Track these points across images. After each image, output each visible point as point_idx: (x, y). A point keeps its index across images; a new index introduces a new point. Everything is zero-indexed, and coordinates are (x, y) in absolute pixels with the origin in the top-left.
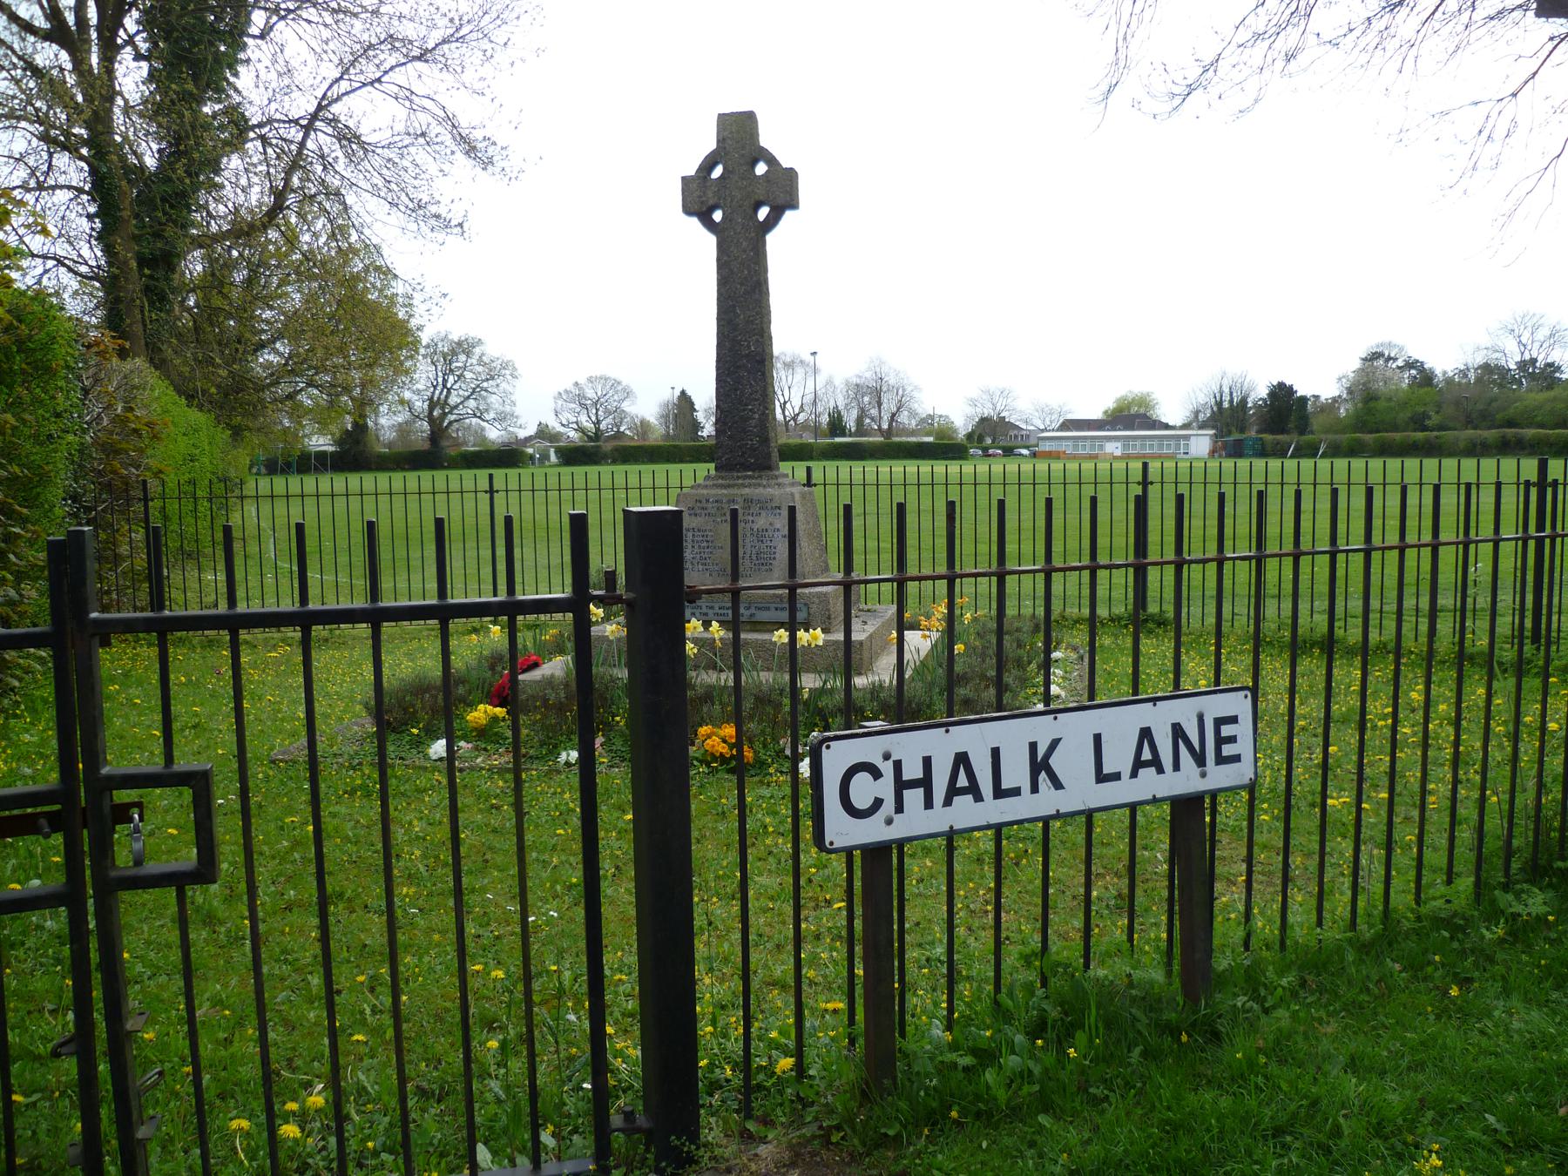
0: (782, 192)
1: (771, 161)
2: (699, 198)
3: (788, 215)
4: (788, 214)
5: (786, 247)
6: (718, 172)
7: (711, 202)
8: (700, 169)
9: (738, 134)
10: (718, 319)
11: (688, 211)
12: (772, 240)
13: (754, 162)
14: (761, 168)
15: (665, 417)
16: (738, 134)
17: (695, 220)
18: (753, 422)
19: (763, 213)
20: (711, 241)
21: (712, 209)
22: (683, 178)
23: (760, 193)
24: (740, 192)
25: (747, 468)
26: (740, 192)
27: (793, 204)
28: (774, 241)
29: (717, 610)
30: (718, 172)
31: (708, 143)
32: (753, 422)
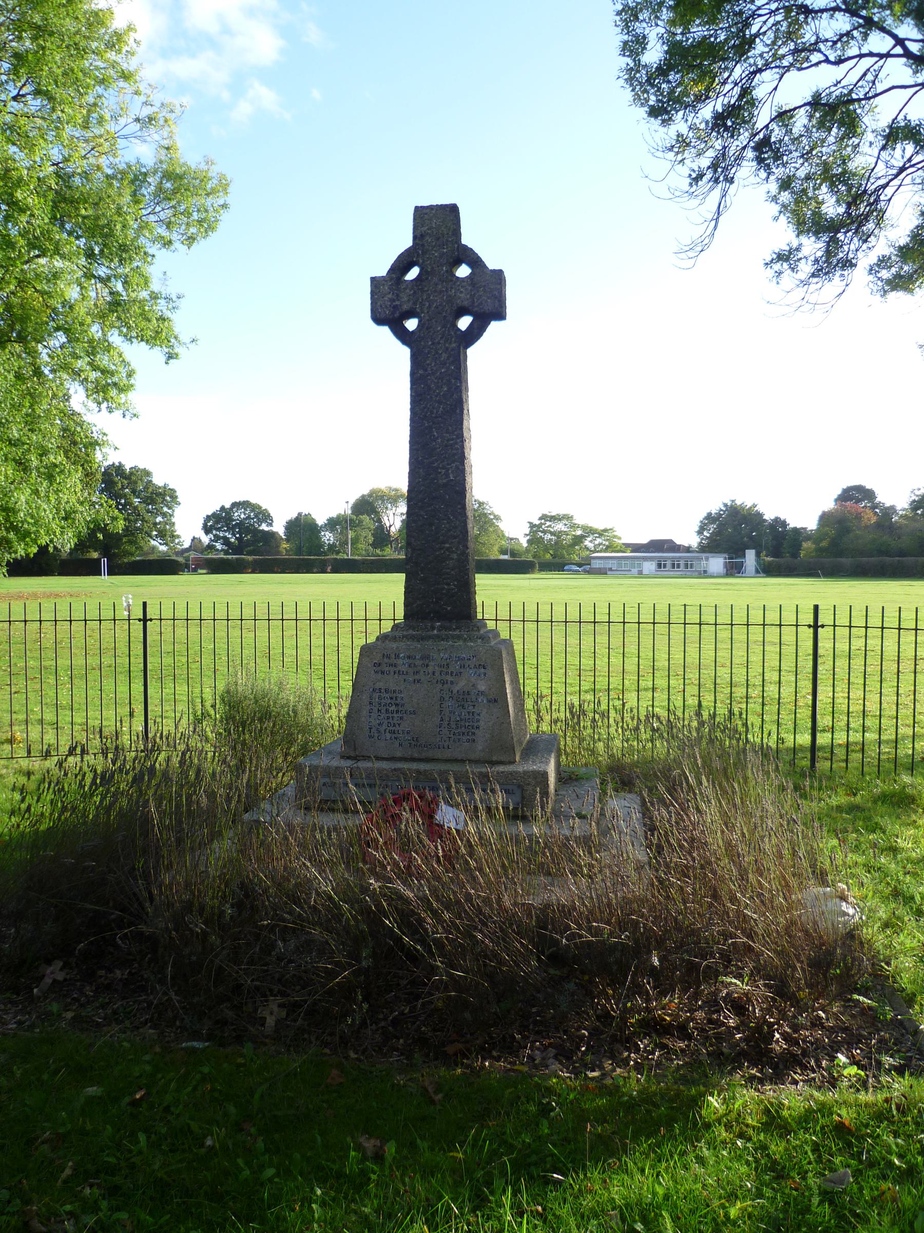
0: (486, 299)
1: (475, 261)
2: (390, 303)
3: (494, 327)
4: (494, 326)
6: (413, 273)
7: (405, 307)
8: (392, 270)
9: (437, 230)
10: (410, 442)
11: (378, 319)
12: (475, 354)
13: (458, 263)
14: (463, 271)
16: (437, 230)
17: (385, 330)
18: (451, 563)
19: (464, 323)
21: (409, 315)
22: (373, 280)
23: (463, 298)
24: (438, 296)
25: (440, 616)
26: (438, 296)
27: (500, 314)
28: (477, 357)
30: (413, 273)
31: (403, 239)
32: (451, 563)
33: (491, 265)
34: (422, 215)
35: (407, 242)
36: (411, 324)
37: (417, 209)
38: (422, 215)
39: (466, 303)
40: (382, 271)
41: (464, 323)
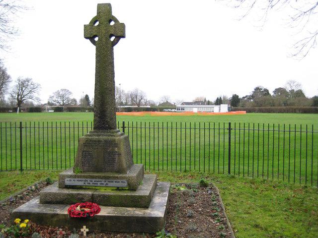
0: (119, 33)
1: (116, 21)
4: (122, 40)
5: (120, 50)
6: (97, 24)
9: (105, 12)
13: (110, 21)
14: (112, 23)
15: (81, 100)
16: (105, 12)
20: (94, 47)
21: (95, 36)
24: (105, 32)
26: (105, 32)
28: (116, 49)
29: (93, 182)
31: (94, 14)
33: (121, 22)
34: (100, 6)
35: (95, 14)
36: (96, 39)
37: (98, 4)
38: (100, 6)
39: (112, 33)
40: (88, 23)
41: (113, 39)
